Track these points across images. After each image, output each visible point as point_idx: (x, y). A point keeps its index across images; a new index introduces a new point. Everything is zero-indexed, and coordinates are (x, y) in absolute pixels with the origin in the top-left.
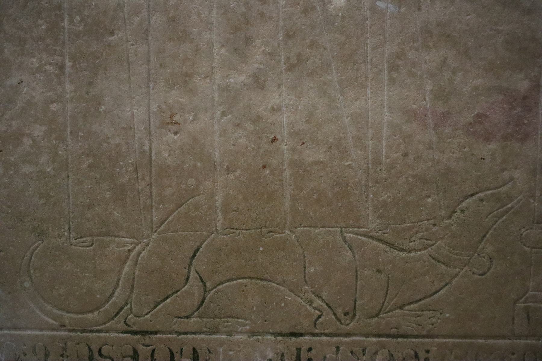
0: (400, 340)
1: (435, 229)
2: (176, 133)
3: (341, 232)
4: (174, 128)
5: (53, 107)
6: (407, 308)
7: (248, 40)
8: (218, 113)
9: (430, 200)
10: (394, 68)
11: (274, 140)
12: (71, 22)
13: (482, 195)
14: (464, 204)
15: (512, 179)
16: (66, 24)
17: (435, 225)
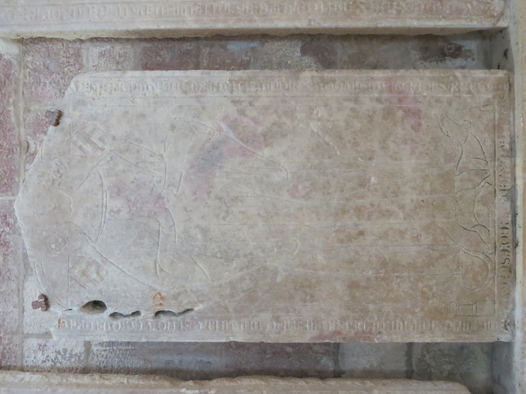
0: (496, 153)
1: (454, 142)
2: (421, 236)
3: (456, 176)
4: (419, 237)
5: (412, 280)
6: (484, 151)
7: (387, 211)
8: (413, 221)
9: (443, 144)
10: (396, 159)
11: (423, 201)
12: (381, 273)
13: (441, 126)
14: (445, 132)
15: (435, 115)
16: (382, 275)
17: (453, 142)
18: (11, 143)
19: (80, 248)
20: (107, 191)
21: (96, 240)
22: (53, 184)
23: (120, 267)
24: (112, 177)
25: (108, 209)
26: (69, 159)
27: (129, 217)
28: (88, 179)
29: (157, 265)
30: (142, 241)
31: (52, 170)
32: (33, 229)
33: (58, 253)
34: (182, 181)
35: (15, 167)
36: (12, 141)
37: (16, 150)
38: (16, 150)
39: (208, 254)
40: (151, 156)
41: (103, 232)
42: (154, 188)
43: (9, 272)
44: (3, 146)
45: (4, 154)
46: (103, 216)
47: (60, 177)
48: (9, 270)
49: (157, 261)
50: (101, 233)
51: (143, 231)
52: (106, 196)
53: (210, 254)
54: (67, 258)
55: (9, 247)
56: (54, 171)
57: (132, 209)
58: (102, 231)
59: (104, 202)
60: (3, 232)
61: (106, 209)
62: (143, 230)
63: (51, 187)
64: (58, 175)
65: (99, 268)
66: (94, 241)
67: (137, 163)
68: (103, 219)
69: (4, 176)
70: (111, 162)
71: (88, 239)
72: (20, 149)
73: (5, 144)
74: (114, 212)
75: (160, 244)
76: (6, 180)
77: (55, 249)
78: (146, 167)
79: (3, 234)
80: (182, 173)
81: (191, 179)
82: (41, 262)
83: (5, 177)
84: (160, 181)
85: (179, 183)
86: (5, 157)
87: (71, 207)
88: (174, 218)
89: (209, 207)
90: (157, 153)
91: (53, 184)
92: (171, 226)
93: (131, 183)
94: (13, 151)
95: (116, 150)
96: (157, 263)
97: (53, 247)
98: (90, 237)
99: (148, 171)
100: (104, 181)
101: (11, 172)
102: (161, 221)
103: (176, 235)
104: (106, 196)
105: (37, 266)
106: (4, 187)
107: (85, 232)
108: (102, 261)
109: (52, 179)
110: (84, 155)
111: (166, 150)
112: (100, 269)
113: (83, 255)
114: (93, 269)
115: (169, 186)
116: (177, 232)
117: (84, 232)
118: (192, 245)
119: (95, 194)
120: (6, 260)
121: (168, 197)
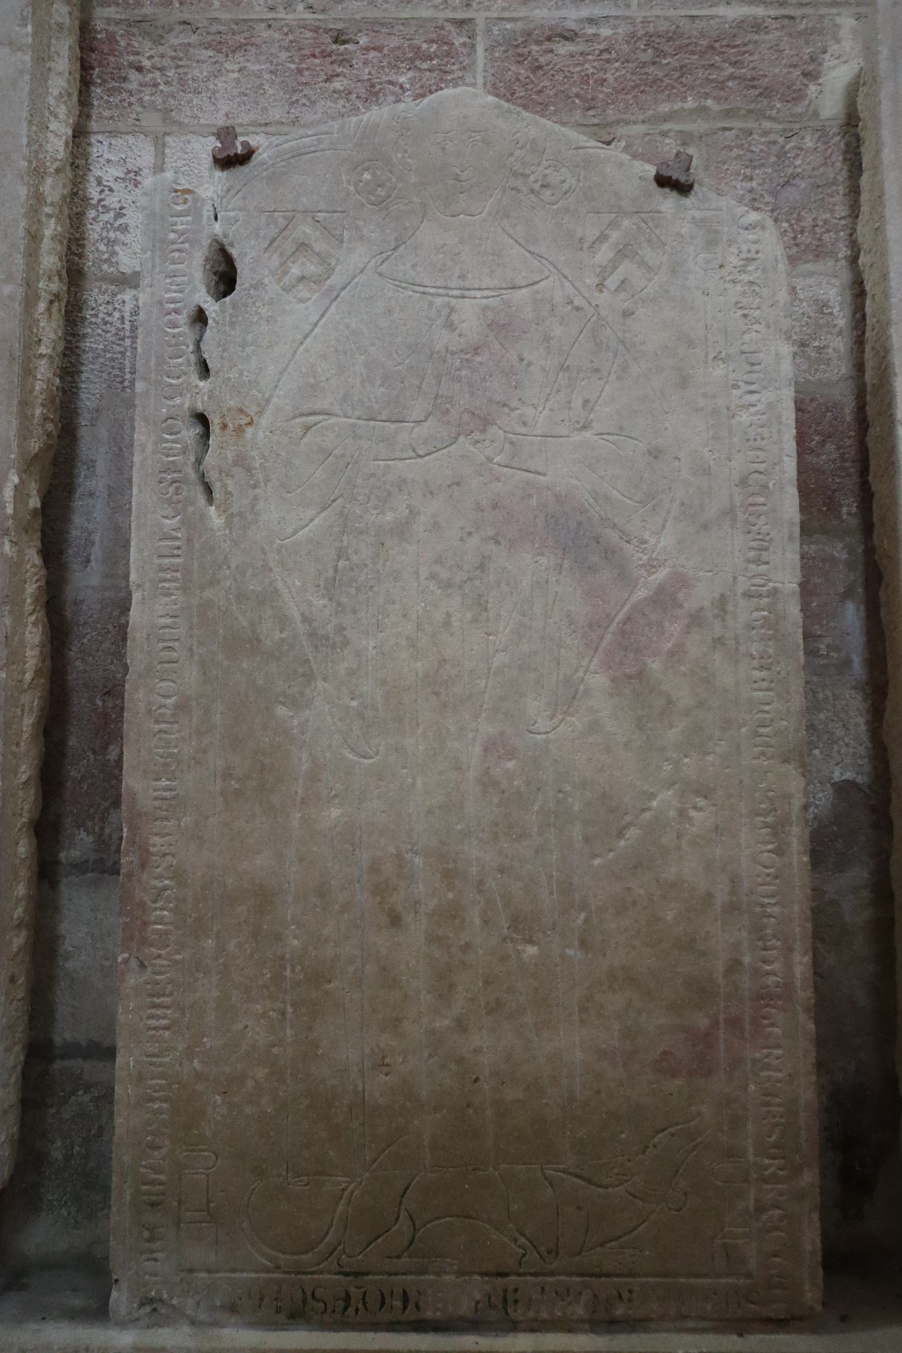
0: (603, 1279)
1: (629, 1164)
2: (387, 1075)
3: (542, 1169)
4: (385, 1070)
5: (275, 1050)
6: (609, 1245)
7: (451, 987)
8: (426, 1054)
9: (623, 1136)
10: (583, 1010)
11: (476, 1080)
12: (293, 971)
13: (672, 1130)
14: (656, 1140)
15: (699, 1113)
16: (288, 973)
17: (629, 1160)
21: (380, 275)
22: (516, 174)
23: (316, 330)
24: (534, 310)
27: (437, 349)
28: (527, 254)
29: (321, 417)
31: (547, 171)
32: (408, 130)
33: (352, 188)
34: (527, 474)
36: (612, 107)
38: (594, 116)
39: (345, 538)
40: (586, 402)
42: (506, 410)
47: (532, 191)
48: (313, 103)
50: (397, 286)
51: (402, 383)
52: (488, 297)
54: (339, 209)
56: (546, 176)
58: (404, 288)
59: (473, 293)
61: (457, 297)
64: (537, 186)
67: (568, 366)
68: (431, 290)
70: (569, 307)
71: (384, 255)
74: (450, 314)
75: (372, 423)
77: (361, 181)
78: (559, 391)
80: (544, 475)
84: (525, 424)
85: (519, 469)
87: (462, 216)
88: (433, 455)
89: (461, 539)
90: (592, 416)
91: (516, 174)
92: (414, 450)
93: (519, 356)
94: (589, 109)
96: (326, 417)
97: (365, 176)
98: (388, 261)
100: (524, 290)
102: (426, 424)
103: (394, 462)
104: (488, 297)
108: (331, 289)
109: (527, 172)
110: (586, 245)
113: (345, 245)
114: (313, 268)
115: (512, 443)
116: (400, 464)
117: (400, 246)
119: (491, 271)
120: (336, 95)
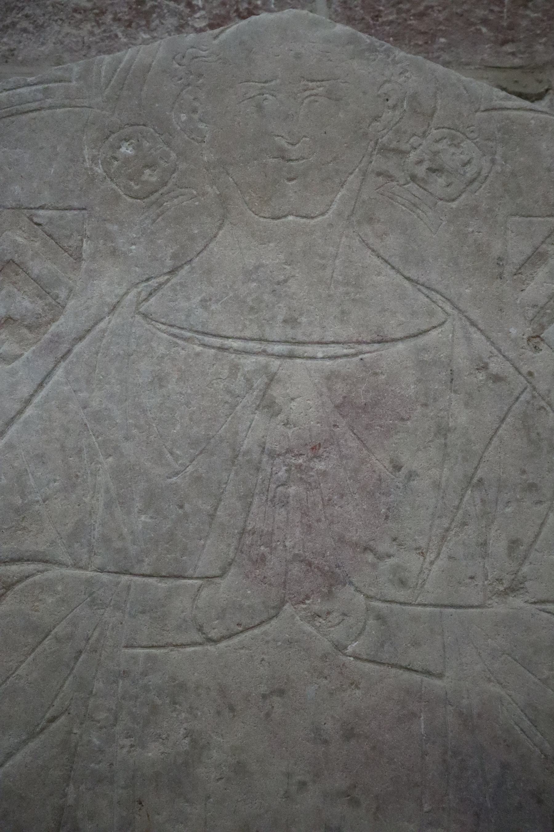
18: (538, 35)
19: (114, 252)
20: (356, 359)
21: (145, 316)
22: (385, 150)
23: (29, 411)
24: (419, 381)
25: (278, 362)
26: (490, 210)
27: (244, 447)
28: (406, 284)
29: (30, 567)
30: (138, 505)
31: (440, 146)
32: (200, 75)
33: (99, 170)
34: (406, 675)
35: (442, 49)
36: (544, 40)
37: (513, 54)
38: (513, 54)
39: (71, 789)
40: (514, 544)
41: (179, 342)
42: (370, 557)
43: (31, 28)
44: (526, 7)
45: (492, 11)
46: (251, 345)
47: (413, 178)
48: (40, 27)
49: (49, 566)
50: (175, 336)
51: (181, 507)
52: (335, 357)
53: (70, 800)
54: (76, 204)
55: (130, 26)
56: (436, 153)
57: (278, 461)
58: (186, 339)
59: (310, 350)
60: (189, 5)
61: (280, 356)
62: (187, 506)
63: (372, 143)
64: (421, 171)
65: (29, 327)
66: (142, 310)
67: (480, 480)
68: (236, 344)
69: (408, 11)
70: (481, 376)
71: (153, 283)
72: (515, 68)
73: (533, 15)
74: (268, 385)
75: (125, 578)
76: (391, 18)
77: (116, 159)
78: (465, 524)
79: (182, 7)
80: (440, 676)
81: (414, 715)
82: (64, 106)
83: (404, 15)
84: (403, 583)
85: (393, 666)
86: (481, 12)
87: (290, 218)
88: (236, 640)
89: (287, 795)
90: (525, 569)
91: (385, 150)
92: (200, 629)
93: (391, 461)
94: (505, 42)
95: (534, 397)
96: (40, 566)
97: (123, 150)
98: (160, 293)
99: (447, 530)
100: (400, 346)
101: (425, 33)
102: (223, 583)
103: (162, 651)
104: (335, 357)
105: (47, 89)
106: (363, 8)
107: (183, 272)
108: (57, 339)
109: (405, 147)
110: (509, 269)
111: (543, 607)
112: (25, 331)
113: (84, 265)
114: (26, 303)
115: (379, 617)
116: (175, 654)
117: (181, 267)
118: (116, 719)
119: (343, 312)
120: (78, 16)
121: (330, 618)
